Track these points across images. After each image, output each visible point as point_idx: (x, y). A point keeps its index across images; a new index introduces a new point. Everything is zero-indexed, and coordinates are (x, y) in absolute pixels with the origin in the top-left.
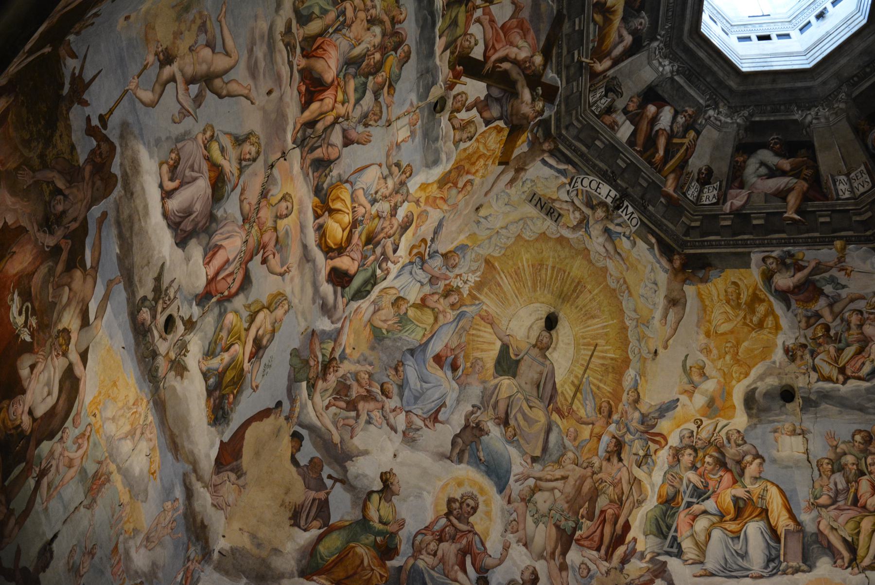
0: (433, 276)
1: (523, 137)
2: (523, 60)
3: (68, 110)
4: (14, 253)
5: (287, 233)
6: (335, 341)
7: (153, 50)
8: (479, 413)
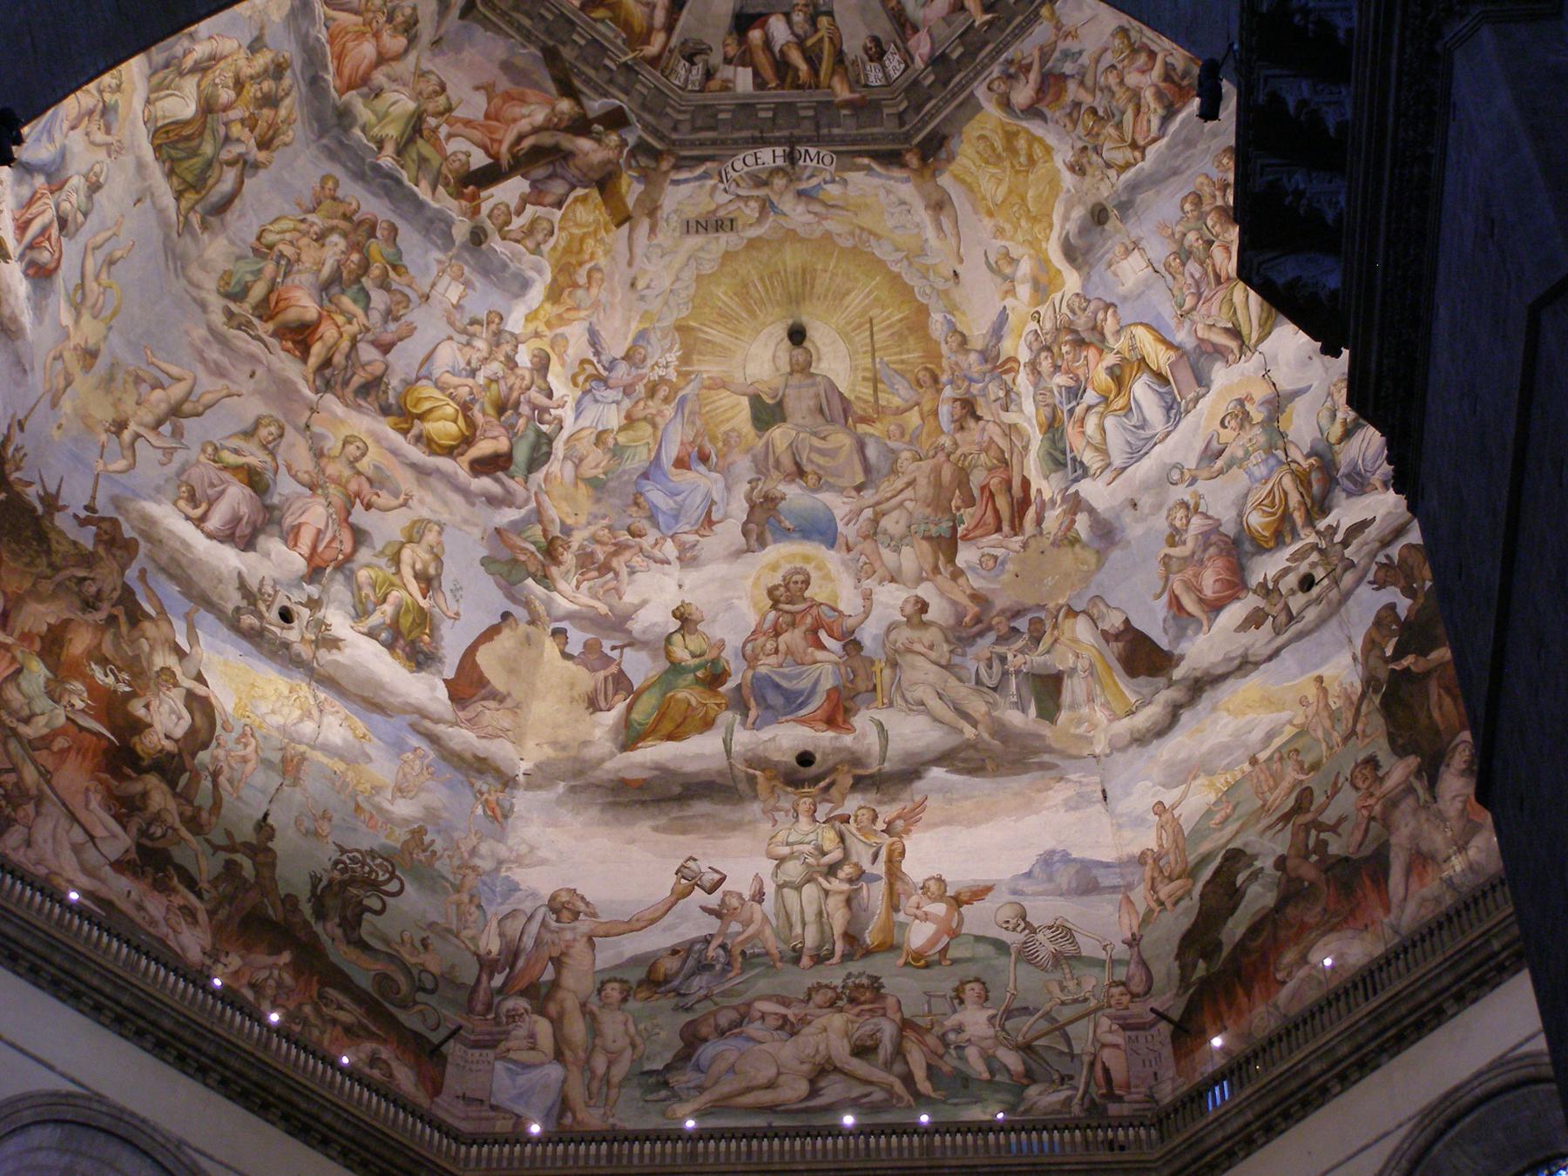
1: (625, 181)
3: (52, 522)
5: (376, 467)
6: (540, 522)
7: (100, 429)
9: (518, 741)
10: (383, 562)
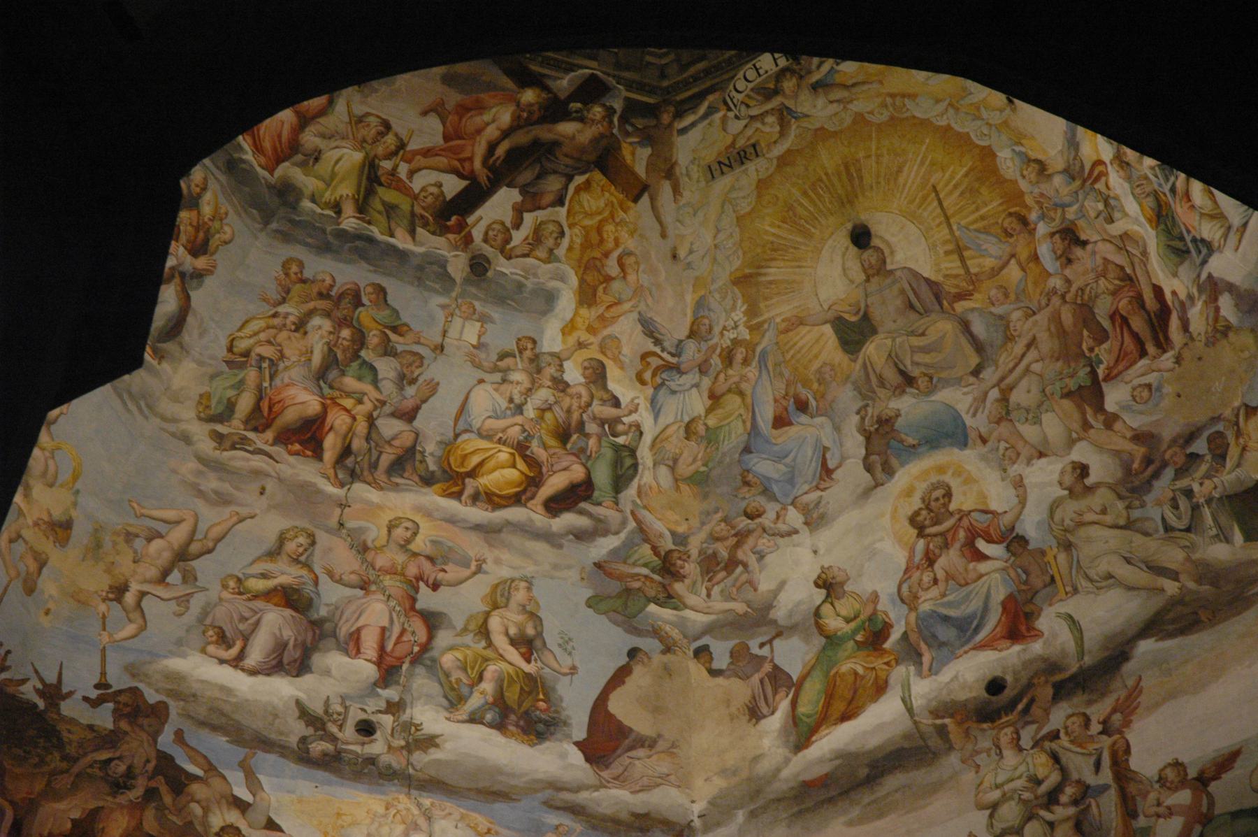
0: (700, 366)
1: (626, 151)
2: (513, 120)
3: (59, 714)
4: (103, 828)
5: (433, 542)
8: (870, 410)
9: (684, 784)
10: (468, 639)
